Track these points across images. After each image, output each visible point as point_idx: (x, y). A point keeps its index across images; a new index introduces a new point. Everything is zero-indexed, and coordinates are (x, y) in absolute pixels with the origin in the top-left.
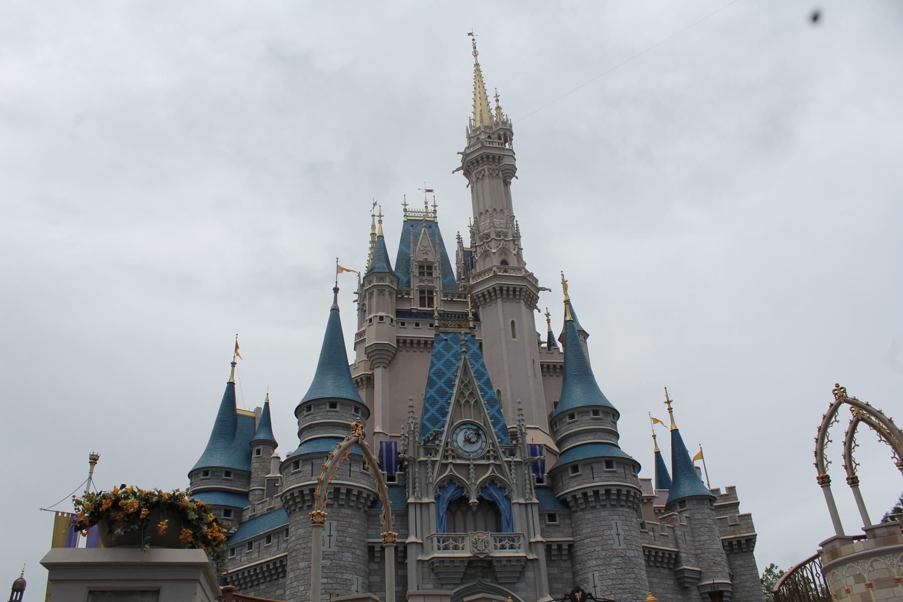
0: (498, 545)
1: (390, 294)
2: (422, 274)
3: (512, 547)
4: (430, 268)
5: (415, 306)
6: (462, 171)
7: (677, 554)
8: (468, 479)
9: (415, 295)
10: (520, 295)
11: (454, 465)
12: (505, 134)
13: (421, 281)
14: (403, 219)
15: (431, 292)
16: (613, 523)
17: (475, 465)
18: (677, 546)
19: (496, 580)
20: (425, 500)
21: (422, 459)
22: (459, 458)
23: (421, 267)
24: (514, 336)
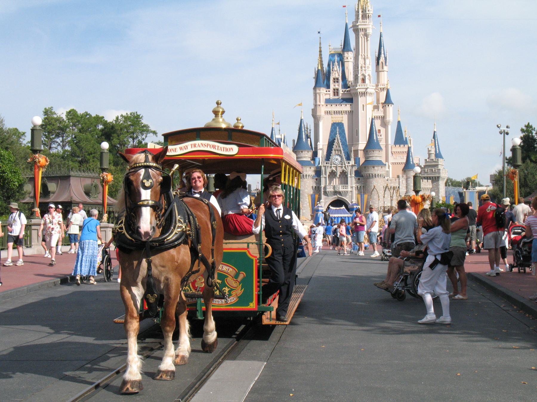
0: (342, 188)
1: (322, 95)
2: (334, 82)
3: (346, 188)
4: (338, 79)
5: (332, 97)
6: (352, 28)
7: (399, 187)
8: (337, 170)
9: (331, 92)
10: (366, 94)
11: (333, 167)
12: (368, 15)
13: (335, 86)
14: (329, 53)
15: (337, 90)
16: (373, 182)
17: (339, 167)
18: (399, 185)
19: (342, 196)
20: (325, 176)
21: (325, 165)
22: (335, 164)
23: (334, 79)
24: (363, 110)
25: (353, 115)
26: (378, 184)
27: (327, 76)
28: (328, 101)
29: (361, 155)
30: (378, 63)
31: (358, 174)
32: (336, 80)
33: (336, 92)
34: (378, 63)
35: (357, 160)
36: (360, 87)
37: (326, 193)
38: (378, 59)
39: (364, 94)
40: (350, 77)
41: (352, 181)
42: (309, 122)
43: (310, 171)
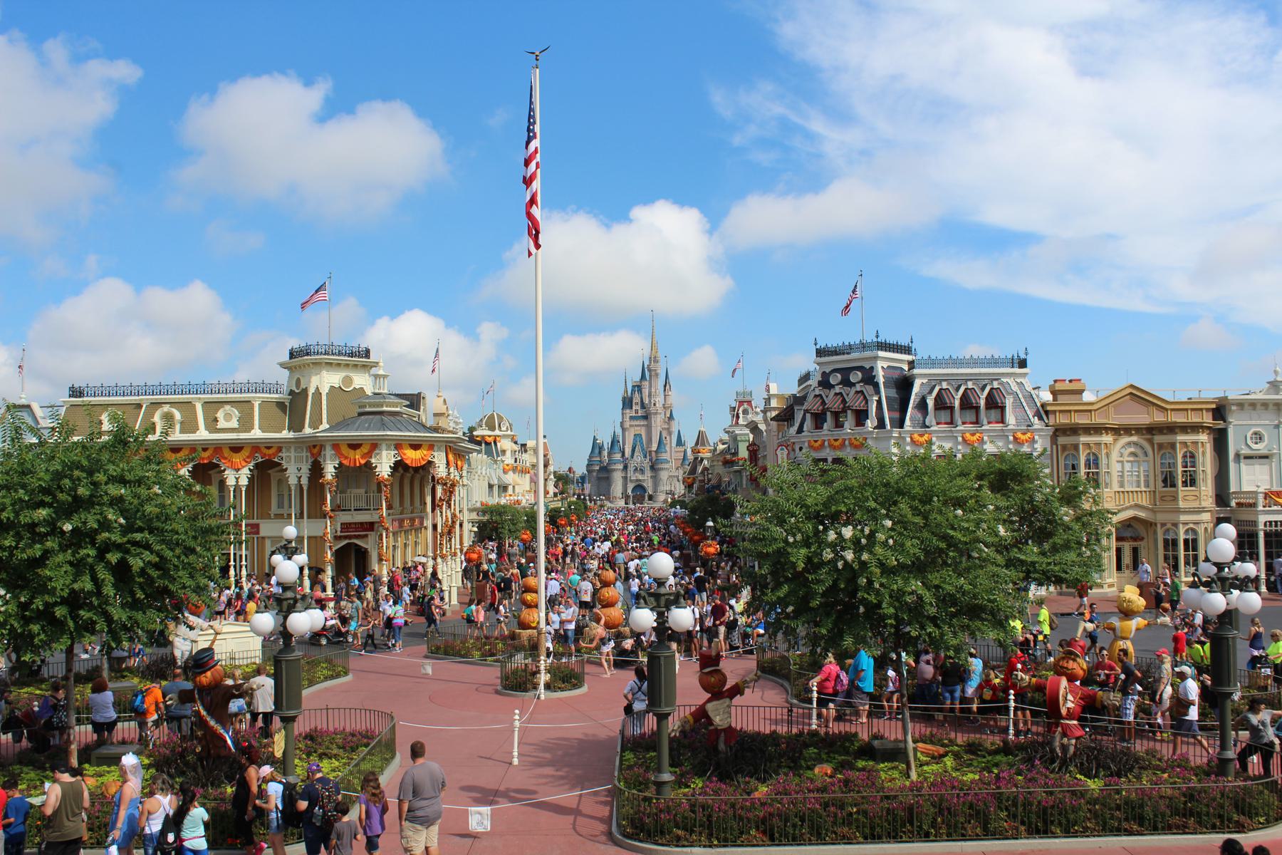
25: (649, 428)
26: (664, 475)
27: (631, 400)
28: (632, 418)
29: (653, 454)
30: (665, 390)
31: (653, 468)
32: (637, 404)
33: (637, 412)
34: (665, 390)
35: (651, 460)
36: (652, 409)
37: (631, 481)
38: (665, 386)
39: (656, 413)
40: (646, 401)
41: (648, 473)
42: (619, 431)
43: (621, 467)
